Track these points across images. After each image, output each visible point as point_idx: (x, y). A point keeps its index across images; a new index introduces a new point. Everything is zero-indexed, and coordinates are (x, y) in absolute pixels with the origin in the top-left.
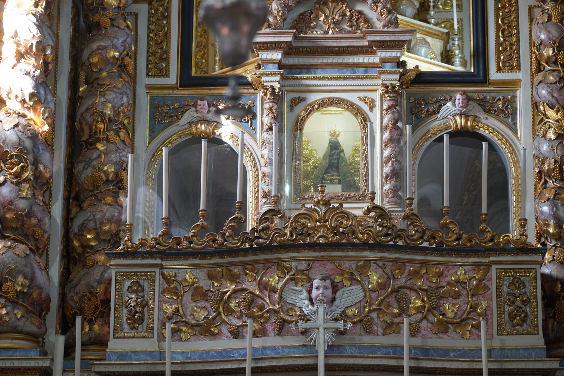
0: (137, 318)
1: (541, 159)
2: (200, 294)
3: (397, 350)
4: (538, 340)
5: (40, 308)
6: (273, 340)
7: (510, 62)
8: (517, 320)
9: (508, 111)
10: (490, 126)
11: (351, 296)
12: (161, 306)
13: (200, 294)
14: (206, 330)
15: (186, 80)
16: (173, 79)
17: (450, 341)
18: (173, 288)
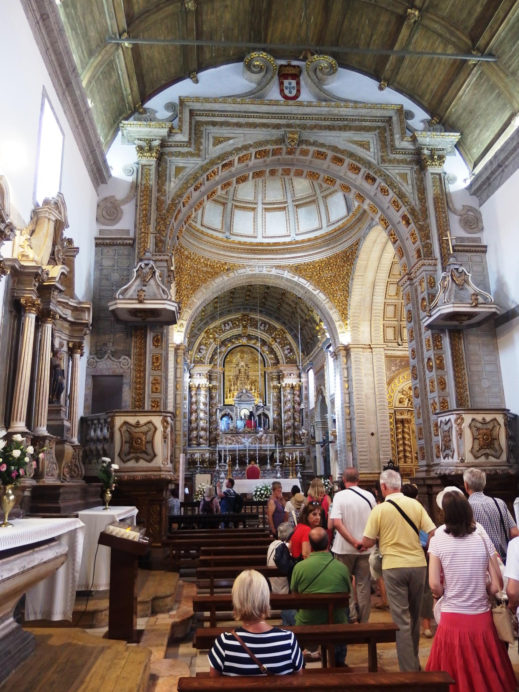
0: (221, 442)
1: (274, 419)
2: (230, 439)
3: (256, 447)
4: (274, 445)
5: (206, 440)
6: (240, 446)
7: (269, 403)
8: (271, 443)
9: (269, 410)
10: (266, 412)
11: (250, 440)
12: (225, 441)
13: (230, 439)
14: (231, 444)
15: (224, 405)
16: (222, 405)
17: (262, 445)
18: (226, 438)
